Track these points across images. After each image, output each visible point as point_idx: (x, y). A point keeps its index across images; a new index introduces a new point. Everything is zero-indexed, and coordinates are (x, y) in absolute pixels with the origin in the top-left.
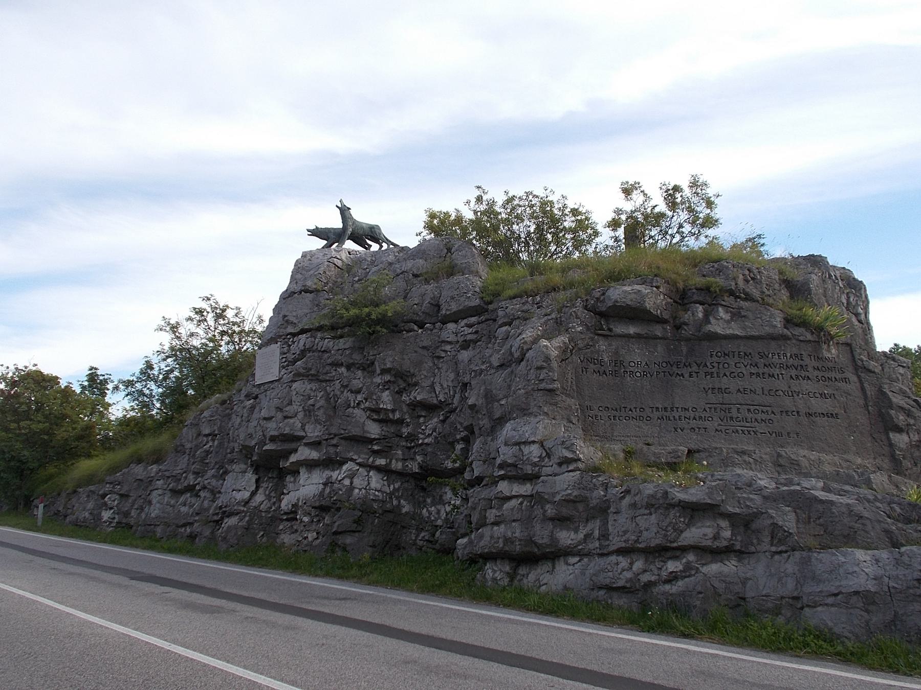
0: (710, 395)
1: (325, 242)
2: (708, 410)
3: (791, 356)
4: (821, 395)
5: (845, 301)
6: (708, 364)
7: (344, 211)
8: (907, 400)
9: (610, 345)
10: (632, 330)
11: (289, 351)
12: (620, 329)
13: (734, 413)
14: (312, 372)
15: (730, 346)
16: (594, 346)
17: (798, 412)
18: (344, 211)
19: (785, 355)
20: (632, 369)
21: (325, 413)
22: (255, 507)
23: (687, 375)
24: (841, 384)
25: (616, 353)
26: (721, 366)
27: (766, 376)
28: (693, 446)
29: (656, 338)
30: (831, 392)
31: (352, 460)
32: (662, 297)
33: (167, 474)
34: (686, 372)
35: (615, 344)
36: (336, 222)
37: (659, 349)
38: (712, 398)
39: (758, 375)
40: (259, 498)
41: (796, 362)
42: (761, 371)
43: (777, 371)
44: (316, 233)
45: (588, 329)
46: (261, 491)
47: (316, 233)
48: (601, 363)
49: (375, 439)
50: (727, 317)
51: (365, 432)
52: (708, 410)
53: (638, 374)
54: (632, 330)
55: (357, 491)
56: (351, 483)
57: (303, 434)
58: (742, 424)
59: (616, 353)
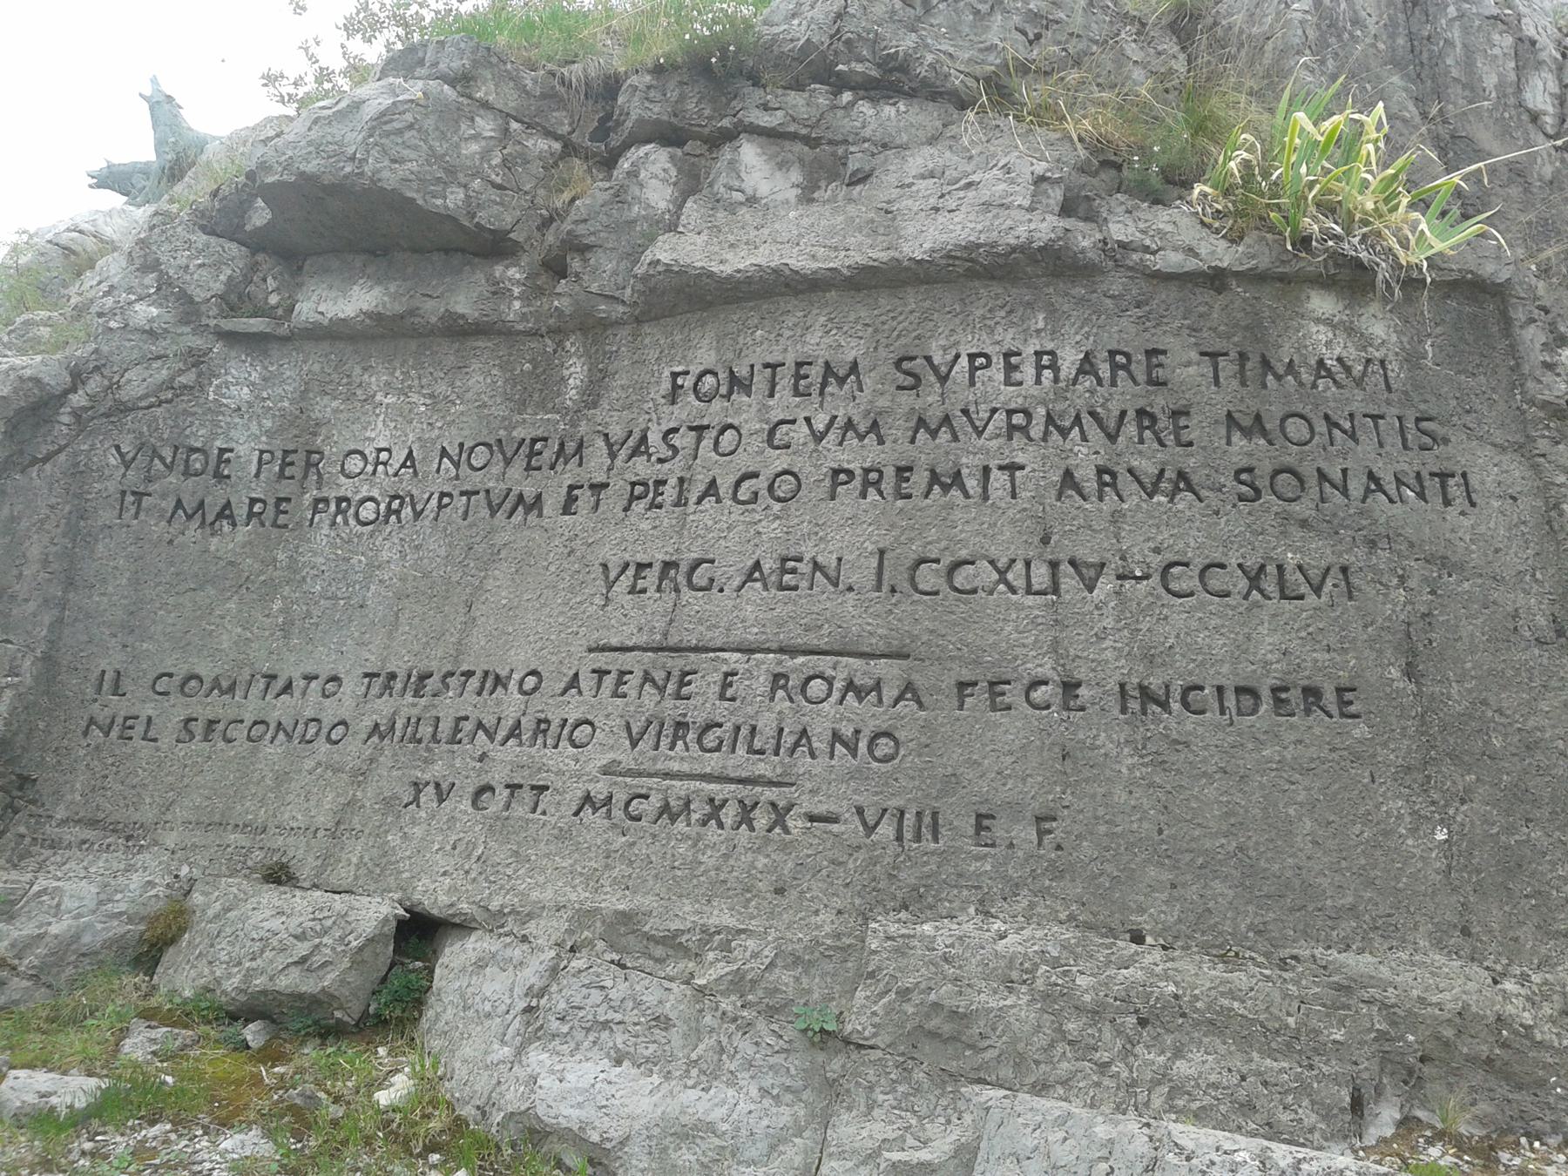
2: (587, 682)
3: (1087, 366)
4: (1255, 578)
6: (654, 438)
10: (354, 300)
13: (703, 703)
15: (763, 343)
17: (1070, 687)
20: (346, 487)
24: (1404, 512)
26: (707, 443)
27: (920, 478)
28: (435, 896)
30: (1318, 552)
35: (291, 370)
38: (636, 617)
39: (871, 479)
43: (992, 446)
45: (188, 310)
47: (112, 179)
52: (587, 682)
53: (367, 512)
54: (354, 300)
58: (712, 763)
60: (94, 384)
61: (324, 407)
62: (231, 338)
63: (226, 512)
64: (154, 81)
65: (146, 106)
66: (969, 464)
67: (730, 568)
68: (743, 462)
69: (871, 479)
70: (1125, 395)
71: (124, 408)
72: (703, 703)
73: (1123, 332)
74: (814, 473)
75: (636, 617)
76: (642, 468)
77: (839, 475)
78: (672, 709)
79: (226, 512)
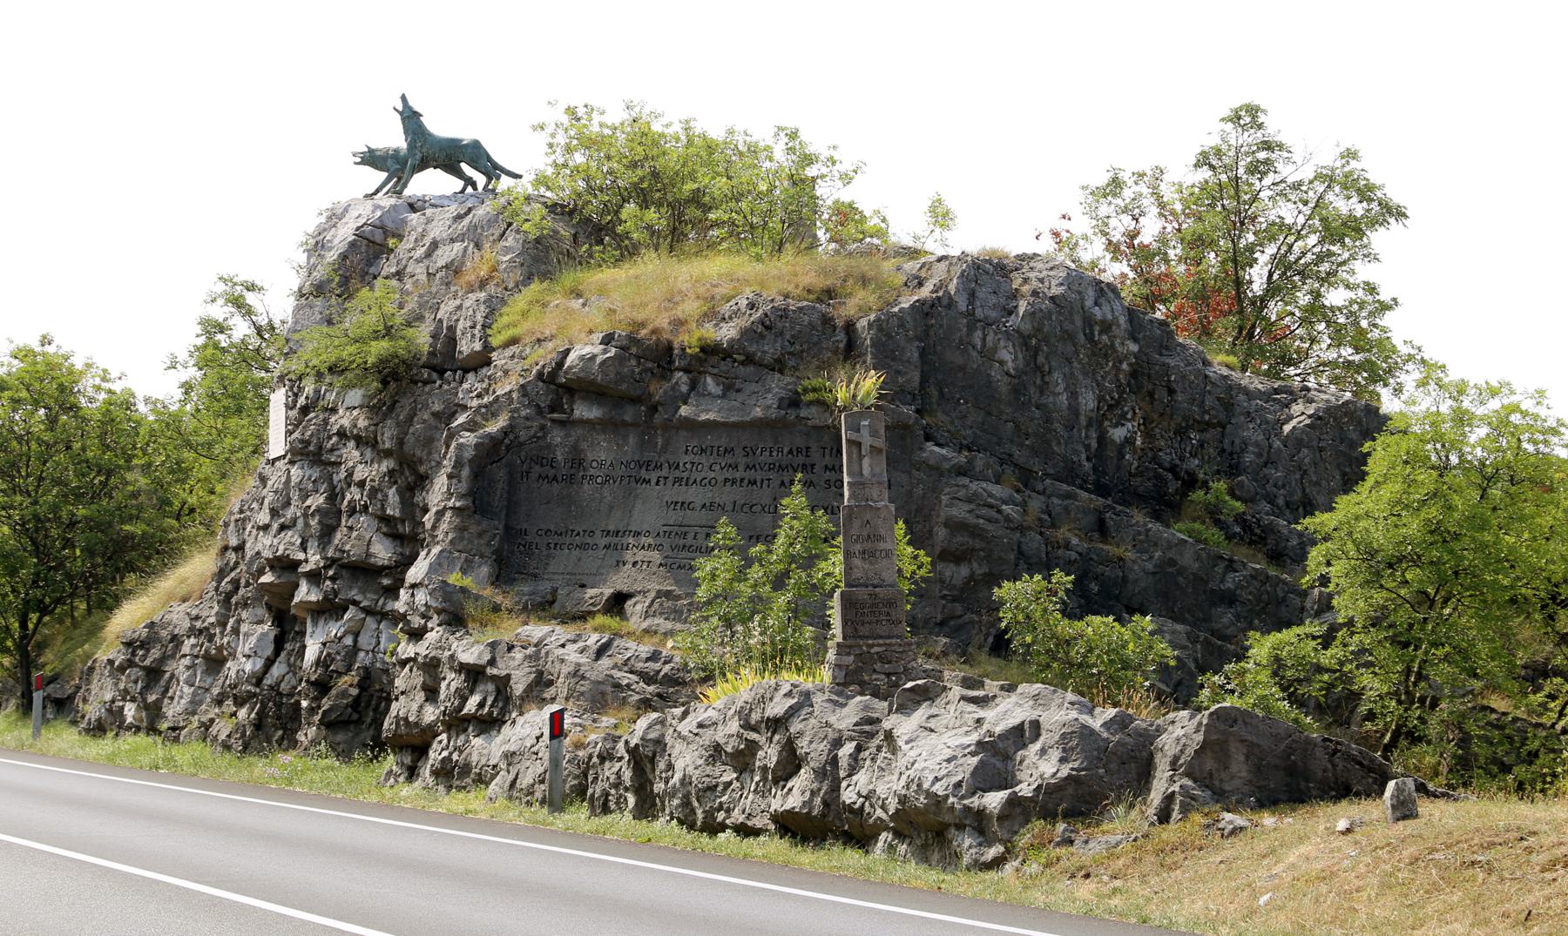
0: (671, 513)
1: (385, 175)
3: (790, 452)
5: (979, 343)
7: (411, 119)
8: (984, 511)
9: (567, 435)
11: (295, 402)
12: (584, 411)
14: (311, 448)
15: (709, 439)
16: (544, 437)
18: (411, 119)
19: (780, 450)
20: (592, 472)
21: (320, 522)
22: (271, 687)
23: (654, 481)
25: (575, 448)
29: (625, 424)
31: (355, 603)
32: (633, 362)
33: (198, 624)
34: (653, 477)
36: (394, 138)
37: (632, 440)
38: (675, 516)
40: (277, 670)
41: (801, 459)
42: (738, 476)
44: (371, 159)
46: (283, 654)
47: (371, 159)
48: (552, 463)
49: (384, 568)
50: (717, 390)
51: (368, 555)
55: (362, 654)
56: (355, 641)
57: (301, 556)
59: (575, 448)
60: (511, 436)
61: (584, 445)
62: (553, 421)
63: (555, 478)
64: (404, 98)
65: (398, 117)
66: (759, 479)
67: (698, 505)
68: (703, 474)
69: (734, 482)
70: (801, 459)
71: (521, 444)
72: (689, 540)
73: (799, 442)
74: (721, 479)
75: (675, 516)
76: (677, 473)
77: (726, 480)
78: (682, 542)
79: (555, 478)
